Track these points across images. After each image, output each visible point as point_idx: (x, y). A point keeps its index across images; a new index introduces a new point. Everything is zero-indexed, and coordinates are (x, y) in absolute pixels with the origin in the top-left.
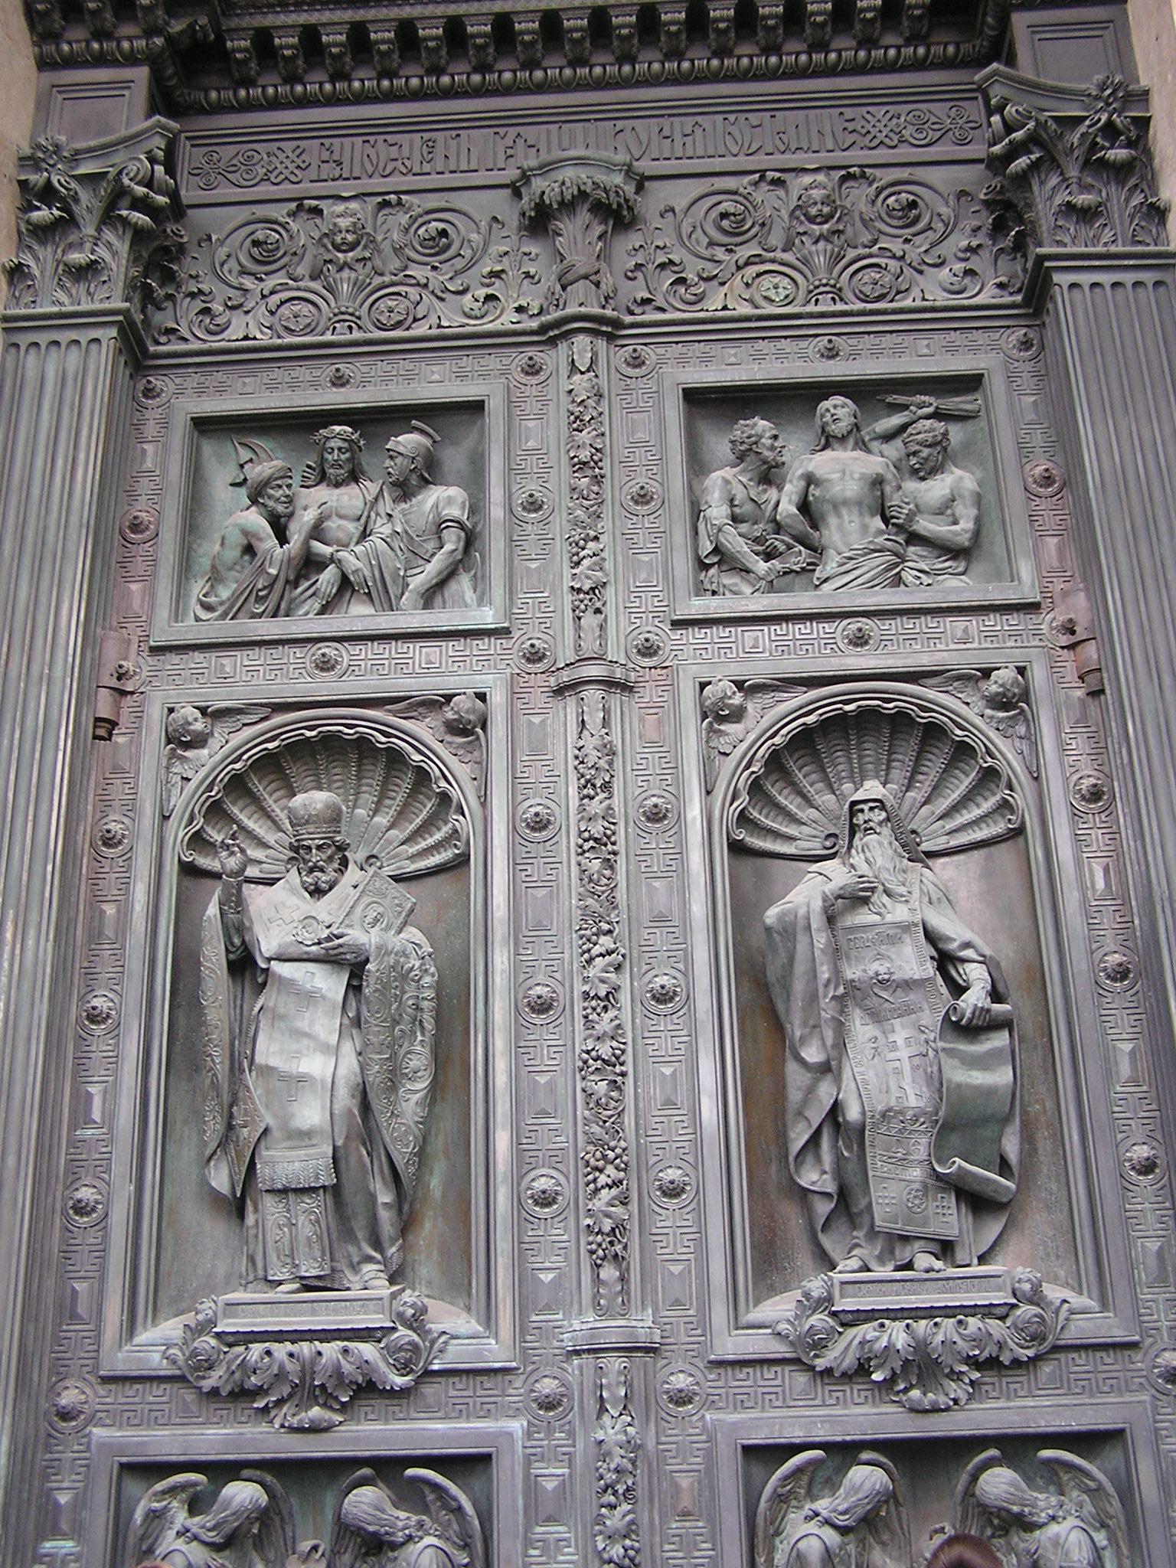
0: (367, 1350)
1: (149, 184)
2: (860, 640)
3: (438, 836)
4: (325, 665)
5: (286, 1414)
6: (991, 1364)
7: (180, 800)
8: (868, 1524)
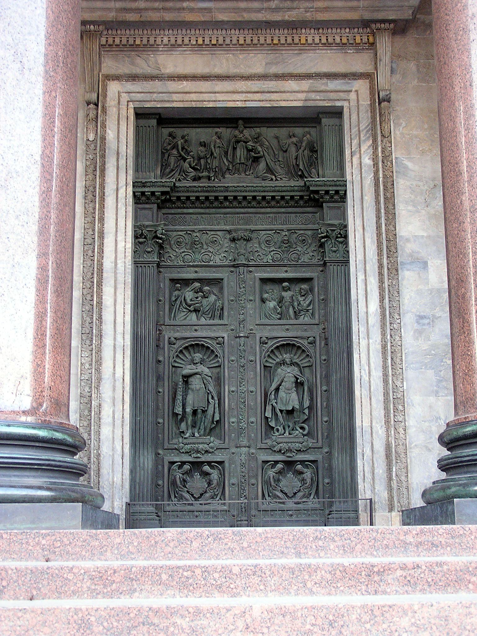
0: (206, 446)
1: (162, 234)
2: (287, 330)
3: (215, 361)
4: (196, 330)
5: (195, 455)
6: (300, 450)
7: (171, 354)
8: (280, 472)
